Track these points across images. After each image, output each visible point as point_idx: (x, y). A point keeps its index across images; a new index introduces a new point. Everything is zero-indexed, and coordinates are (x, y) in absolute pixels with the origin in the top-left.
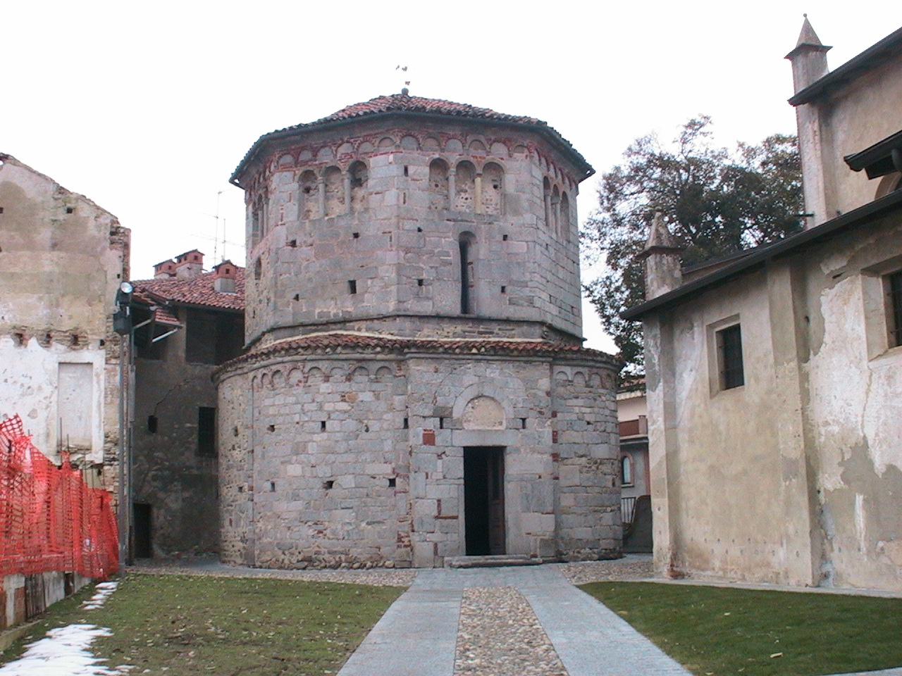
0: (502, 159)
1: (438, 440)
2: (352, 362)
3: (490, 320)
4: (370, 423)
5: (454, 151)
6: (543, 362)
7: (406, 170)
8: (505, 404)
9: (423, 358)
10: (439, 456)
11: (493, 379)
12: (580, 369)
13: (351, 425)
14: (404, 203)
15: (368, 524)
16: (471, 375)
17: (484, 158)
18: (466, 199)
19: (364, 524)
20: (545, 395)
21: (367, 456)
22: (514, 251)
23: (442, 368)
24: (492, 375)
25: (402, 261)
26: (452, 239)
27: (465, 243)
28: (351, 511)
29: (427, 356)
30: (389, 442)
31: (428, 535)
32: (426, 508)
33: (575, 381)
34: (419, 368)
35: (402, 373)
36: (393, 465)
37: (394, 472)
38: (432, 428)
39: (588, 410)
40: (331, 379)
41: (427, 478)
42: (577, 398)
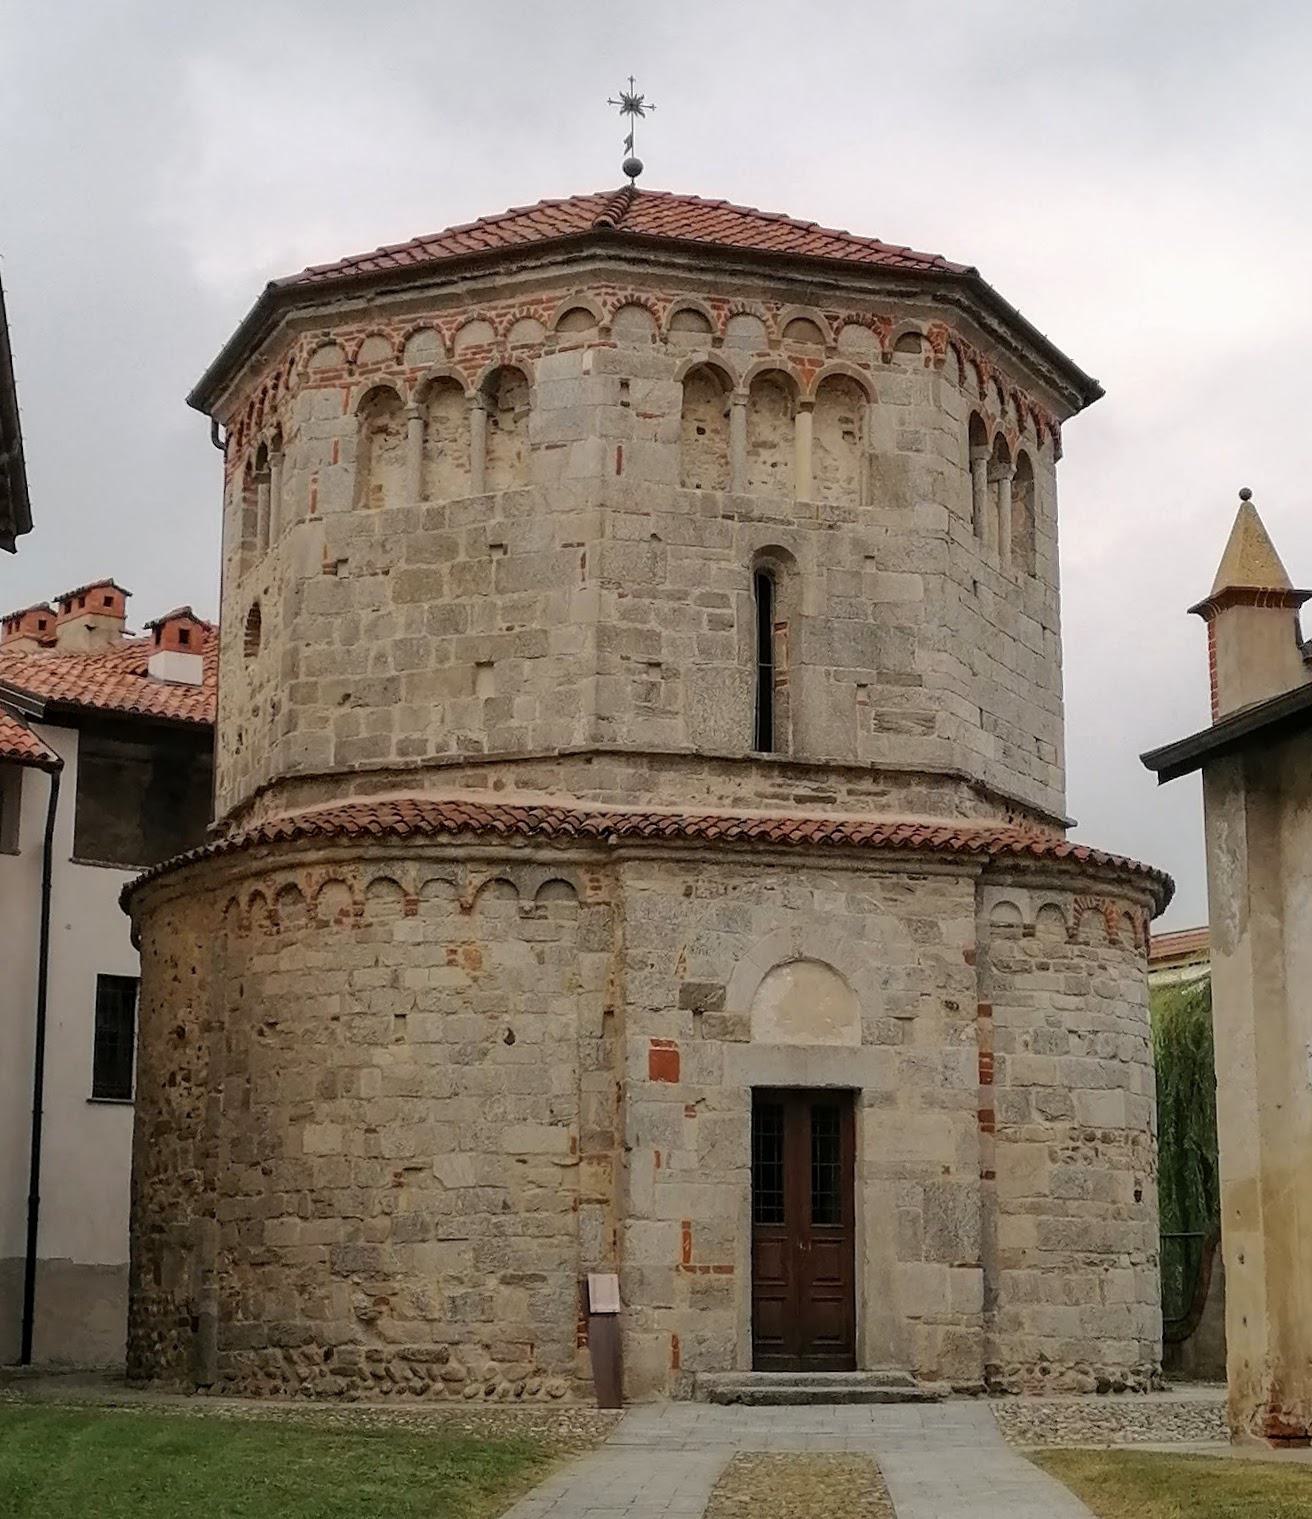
0: (866, 366)
1: (686, 1067)
3: (824, 769)
4: (518, 1022)
14: (618, 472)
15: (505, 1281)
18: (774, 465)
19: (492, 1282)
23: (702, 886)
24: (828, 907)
25: (614, 620)
26: (736, 566)
27: (766, 579)
28: (463, 1245)
29: (666, 854)
30: (566, 1069)
31: (657, 1311)
33: (1040, 927)
34: (642, 884)
35: (603, 895)
37: (573, 1150)
40: (422, 907)
41: (658, 1165)
42: (1044, 967)
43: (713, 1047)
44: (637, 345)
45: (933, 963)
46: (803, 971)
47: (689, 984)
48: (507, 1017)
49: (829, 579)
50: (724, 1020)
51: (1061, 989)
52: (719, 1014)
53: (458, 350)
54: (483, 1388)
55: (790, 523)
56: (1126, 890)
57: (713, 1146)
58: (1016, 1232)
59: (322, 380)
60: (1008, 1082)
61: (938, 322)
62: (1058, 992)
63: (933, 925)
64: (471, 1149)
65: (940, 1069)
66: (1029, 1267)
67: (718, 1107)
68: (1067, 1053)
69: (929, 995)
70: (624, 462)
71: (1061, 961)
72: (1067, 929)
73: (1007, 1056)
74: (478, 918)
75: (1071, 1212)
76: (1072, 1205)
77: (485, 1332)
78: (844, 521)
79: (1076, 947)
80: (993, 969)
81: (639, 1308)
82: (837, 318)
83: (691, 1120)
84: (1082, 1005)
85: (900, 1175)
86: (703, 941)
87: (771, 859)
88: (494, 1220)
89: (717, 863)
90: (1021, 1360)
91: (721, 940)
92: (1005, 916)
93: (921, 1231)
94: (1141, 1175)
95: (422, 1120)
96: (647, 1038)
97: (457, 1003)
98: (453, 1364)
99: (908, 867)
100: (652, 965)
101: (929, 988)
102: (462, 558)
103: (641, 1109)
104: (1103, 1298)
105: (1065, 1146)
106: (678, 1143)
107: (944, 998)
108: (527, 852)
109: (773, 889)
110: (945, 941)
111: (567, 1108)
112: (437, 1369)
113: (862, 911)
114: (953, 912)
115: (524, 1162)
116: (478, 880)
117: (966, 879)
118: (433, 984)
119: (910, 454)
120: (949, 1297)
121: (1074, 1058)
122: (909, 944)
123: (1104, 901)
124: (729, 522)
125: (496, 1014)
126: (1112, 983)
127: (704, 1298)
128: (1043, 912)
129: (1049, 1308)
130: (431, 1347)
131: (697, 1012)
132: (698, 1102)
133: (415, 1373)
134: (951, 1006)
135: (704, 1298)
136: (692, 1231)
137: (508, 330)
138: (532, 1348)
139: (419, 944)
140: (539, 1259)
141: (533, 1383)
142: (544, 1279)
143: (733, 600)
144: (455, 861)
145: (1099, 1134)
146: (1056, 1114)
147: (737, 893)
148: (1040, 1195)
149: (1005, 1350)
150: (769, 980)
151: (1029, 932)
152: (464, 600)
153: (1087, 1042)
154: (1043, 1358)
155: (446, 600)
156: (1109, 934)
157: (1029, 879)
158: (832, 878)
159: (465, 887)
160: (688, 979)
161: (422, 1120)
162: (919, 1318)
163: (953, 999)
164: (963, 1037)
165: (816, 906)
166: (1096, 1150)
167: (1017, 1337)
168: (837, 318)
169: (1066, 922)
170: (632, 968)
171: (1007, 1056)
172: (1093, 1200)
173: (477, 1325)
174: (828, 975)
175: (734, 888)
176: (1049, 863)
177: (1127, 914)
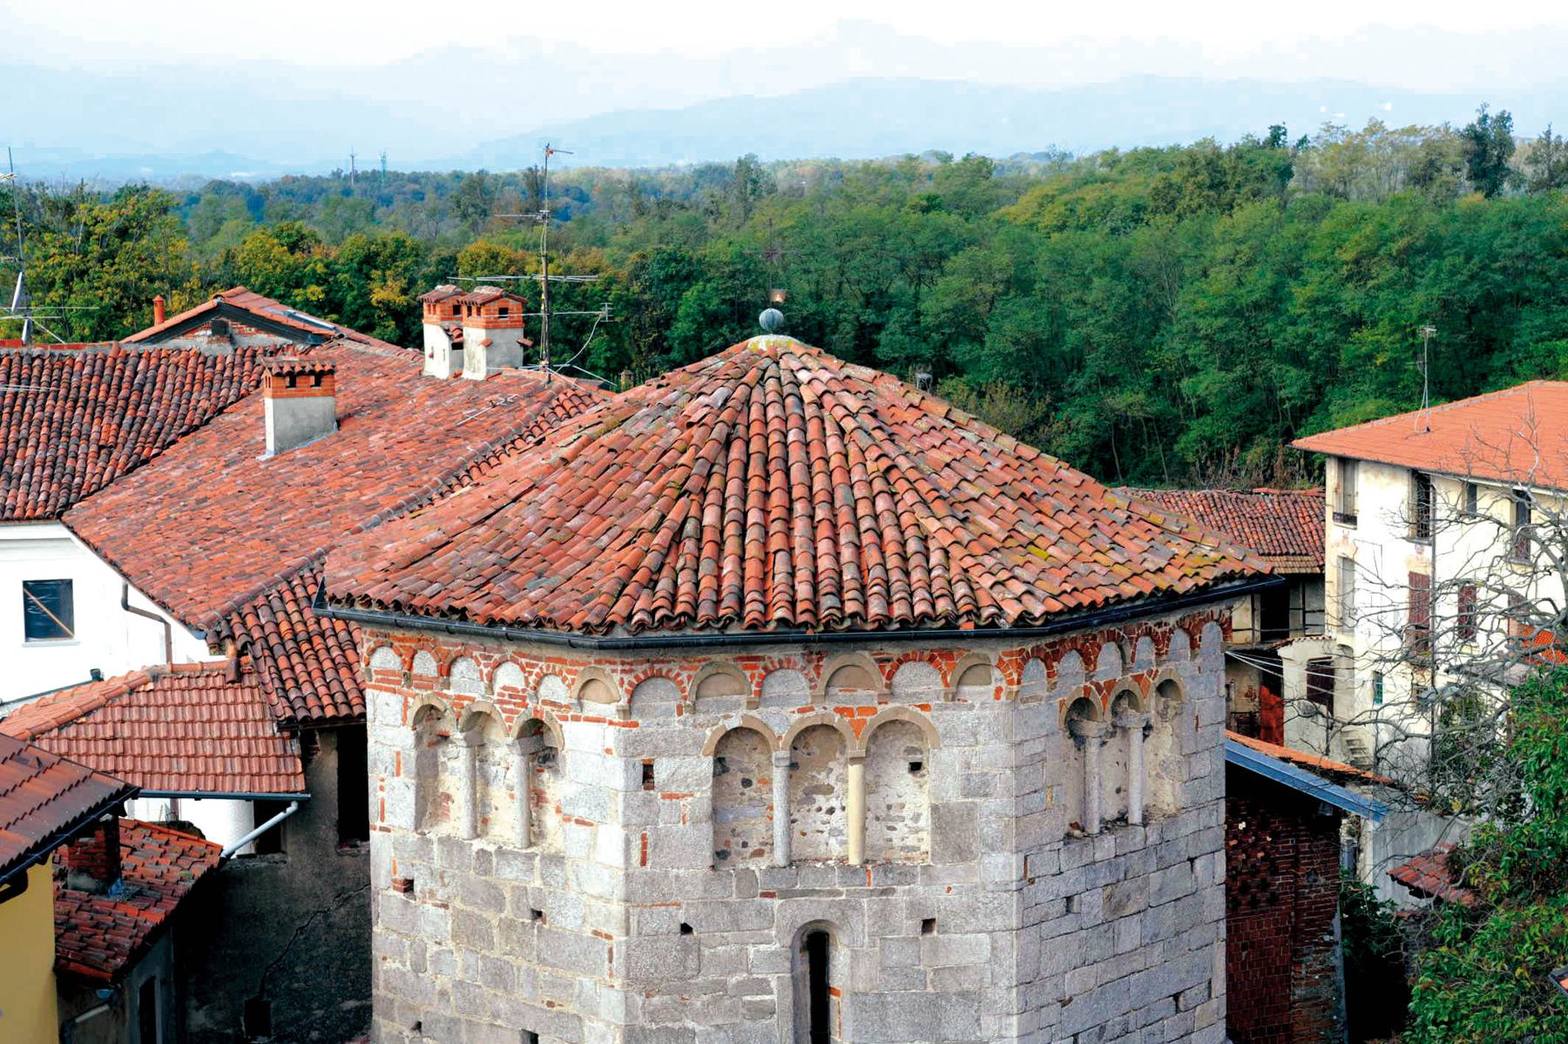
5: (784, 701)
7: (648, 773)
14: (643, 863)
17: (873, 711)
22: (954, 960)
25: (642, 1021)
44: (661, 720)
49: (882, 950)
53: (497, 689)
55: (840, 894)
59: (382, 681)
61: (1008, 649)
70: (649, 851)
78: (900, 883)
82: (888, 660)
102: (508, 913)
119: (977, 800)
124: (768, 900)
137: (538, 683)
143: (773, 984)
152: (510, 958)
155: (496, 954)
168: (888, 660)
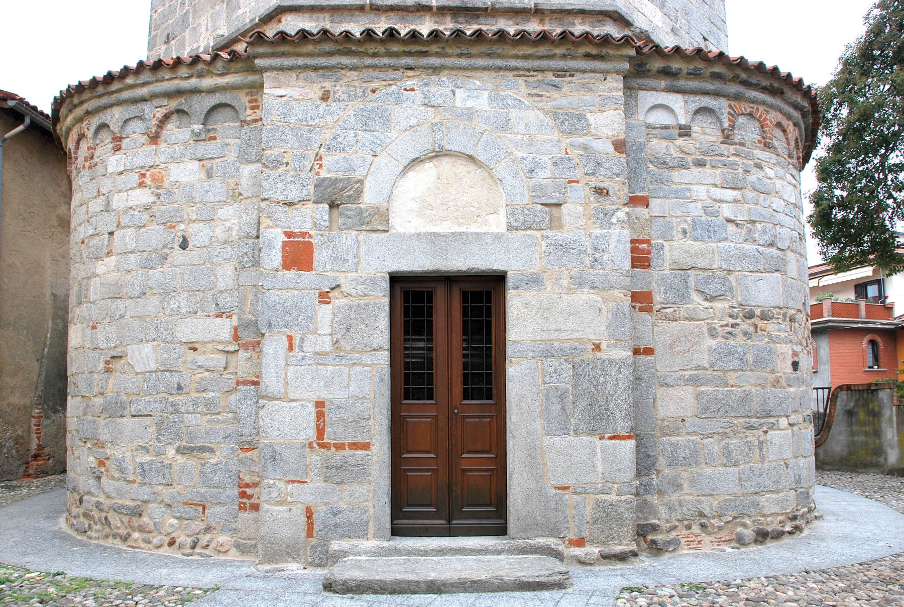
1: (320, 256)
2: (156, 102)
6: (605, 73)
8: (502, 169)
9: (291, 69)
10: (324, 298)
11: (470, 114)
12: (707, 101)
13: (156, 235)
15: (179, 451)
16: (413, 104)
19: (171, 452)
20: (611, 149)
21: (181, 302)
24: (470, 104)
28: (148, 421)
29: (300, 61)
31: (290, 487)
32: (287, 425)
33: (695, 128)
34: (281, 92)
36: (235, 321)
37: (236, 338)
38: (307, 227)
39: (730, 194)
40: (125, 143)
41: (291, 348)
42: (700, 164)
43: (348, 238)
45: (582, 153)
46: (445, 164)
47: (324, 179)
48: (182, 226)
50: (361, 212)
51: (718, 183)
52: (355, 206)
54: (167, 540)
56: (777, 102)
57: (348, 330)
58: (674, 403)
60: (667, 265)
62: (716, 186)
63: (581, 117)
64: (154, 340)
65: (590, 251)
66: (688, 434)
67: (353, 292)
68: (726, 239)
69: (578, 182)
71: (718, 158)
72: (723, 131)
73: (665, 244)
74: (163, 146)
75: (730, 382)
76: (732, 377)
77: (166, 493)
79: (732, 148)
80: (650, 165)
81: (272, 482)
83: (326, 306)
84: (739, 197)
85: (548, 354)
86: (340, 140)
87: (409, 61)
88: (171, 400)
89: (354, 68)
90: (679, 517)
91: (359, 138)
92: (660, 118)
93: (569, 407)
94: (798, 348)
95: (122, 317)
96: (279, 231)
97: (146, 216)
98: (145, 519)
99: (552, 63)
100: (287, 164)
101: (578, 174)
103: (273, 296)
104: (763, 459)
105: (724, 323)
106: (312, 327)
107: (593, 184)
108: (194, 82)
109: (413, 90)
110: (594, 131)
111: (227, 301)
112: (136, 522)
113: (507, 106)
114: (601, 107)
115: (195, 349)
116: (160, 113)
117: (614, 75)
118: (130, 204)
120: (600, 469)
121: (732, 245)
122: (556, 135)
123: (757, 109)
125: (174, 224)
126: (769, 181)
127: (336, 474)
128: (699, 117)
129: (708, 471)
130: (129, 503)
131: (333, 206)
132: (333, 289)
133: (122, 522)
134: (600, 192)
135: (336, 474)
136: (325, 410)
138: (204, 508)
139: (122, 173)
140: (207, 433)
141: (205, 539)
142: (211, 450)
144: (144, 100)
145: (758, 312)
146: (715, 294)
147: (375, 96)
148: (698, 368)
149: (663, 512)
150: (411, 174)
151: (685, 131)
153: (744, 231)
154: (702, 515)
156: (763, 138)
157: (681, 83)
158: (476, 79)
159: (150, 120)
160: (324, 174)
161: (122, 317)
162: (568, 488)
163: (602, 185)
164: (614, 220)
165: (458, 104)
166: (756, 326)
167: (674, 497)
169: (722, 125)
170: (267, 167)
171: (665, 244)
172: (751, 370)
173: (160, 488)
174: (472, 167)
175: (374, 91)
176: (700, 65)
177: (779, 125)
